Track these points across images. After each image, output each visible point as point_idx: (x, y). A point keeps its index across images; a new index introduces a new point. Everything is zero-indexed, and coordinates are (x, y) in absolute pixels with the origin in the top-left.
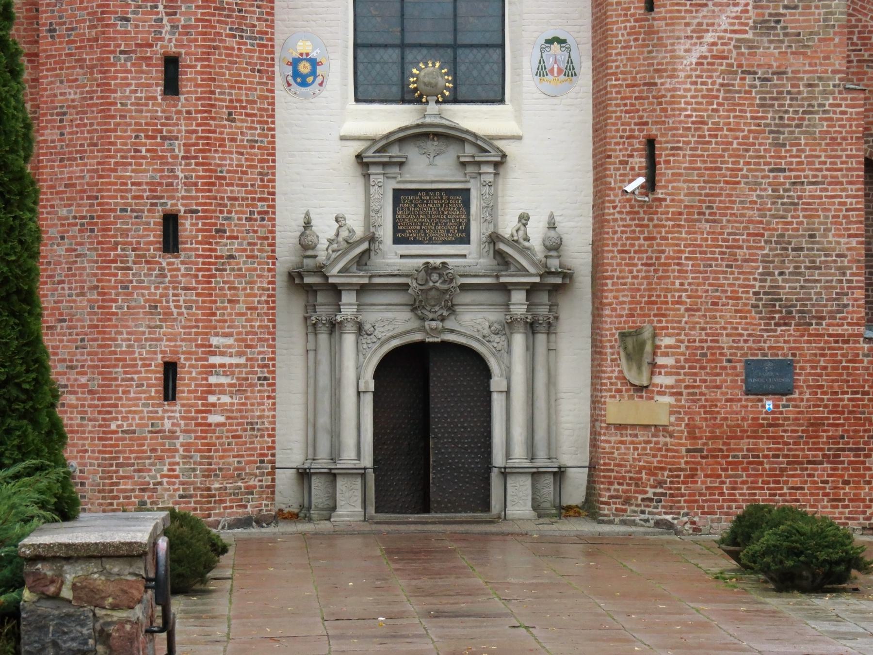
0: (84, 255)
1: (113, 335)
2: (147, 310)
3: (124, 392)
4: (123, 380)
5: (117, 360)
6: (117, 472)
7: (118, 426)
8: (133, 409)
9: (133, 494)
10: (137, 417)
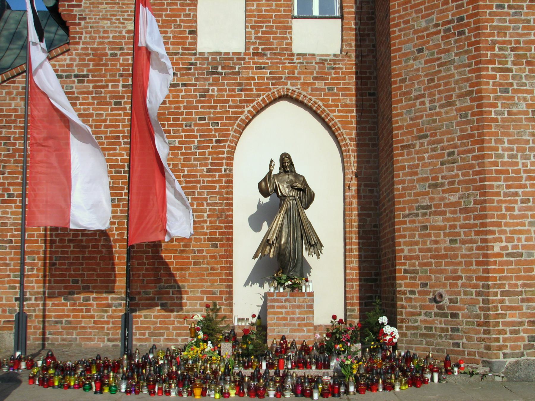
0: (452, 62)
1: (493, 144)
2: (530, 116)
3: (508, 209)
4: (506, 195)
5: (497, 172)
6: (502, 301)
7: (502, 248)
8: (519, 228)
9: (521, 328)
10: (523, 237)
